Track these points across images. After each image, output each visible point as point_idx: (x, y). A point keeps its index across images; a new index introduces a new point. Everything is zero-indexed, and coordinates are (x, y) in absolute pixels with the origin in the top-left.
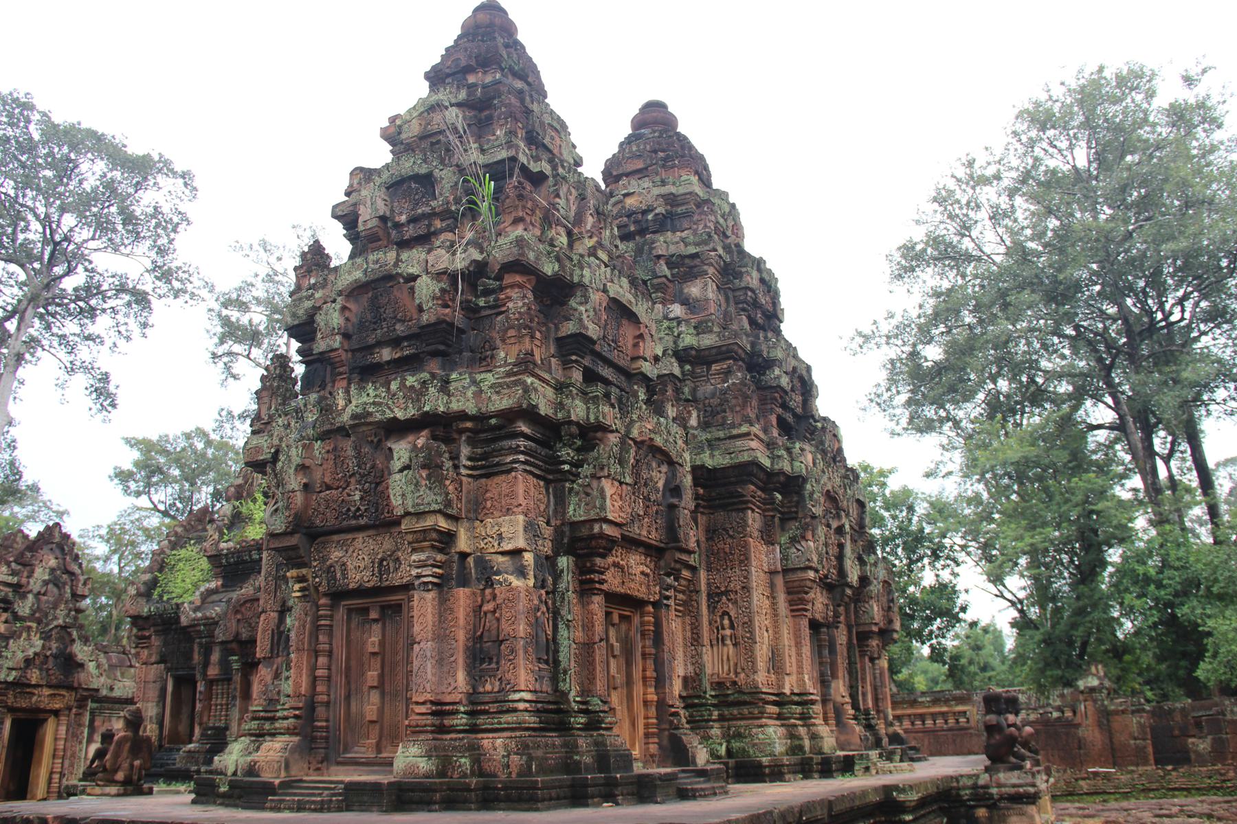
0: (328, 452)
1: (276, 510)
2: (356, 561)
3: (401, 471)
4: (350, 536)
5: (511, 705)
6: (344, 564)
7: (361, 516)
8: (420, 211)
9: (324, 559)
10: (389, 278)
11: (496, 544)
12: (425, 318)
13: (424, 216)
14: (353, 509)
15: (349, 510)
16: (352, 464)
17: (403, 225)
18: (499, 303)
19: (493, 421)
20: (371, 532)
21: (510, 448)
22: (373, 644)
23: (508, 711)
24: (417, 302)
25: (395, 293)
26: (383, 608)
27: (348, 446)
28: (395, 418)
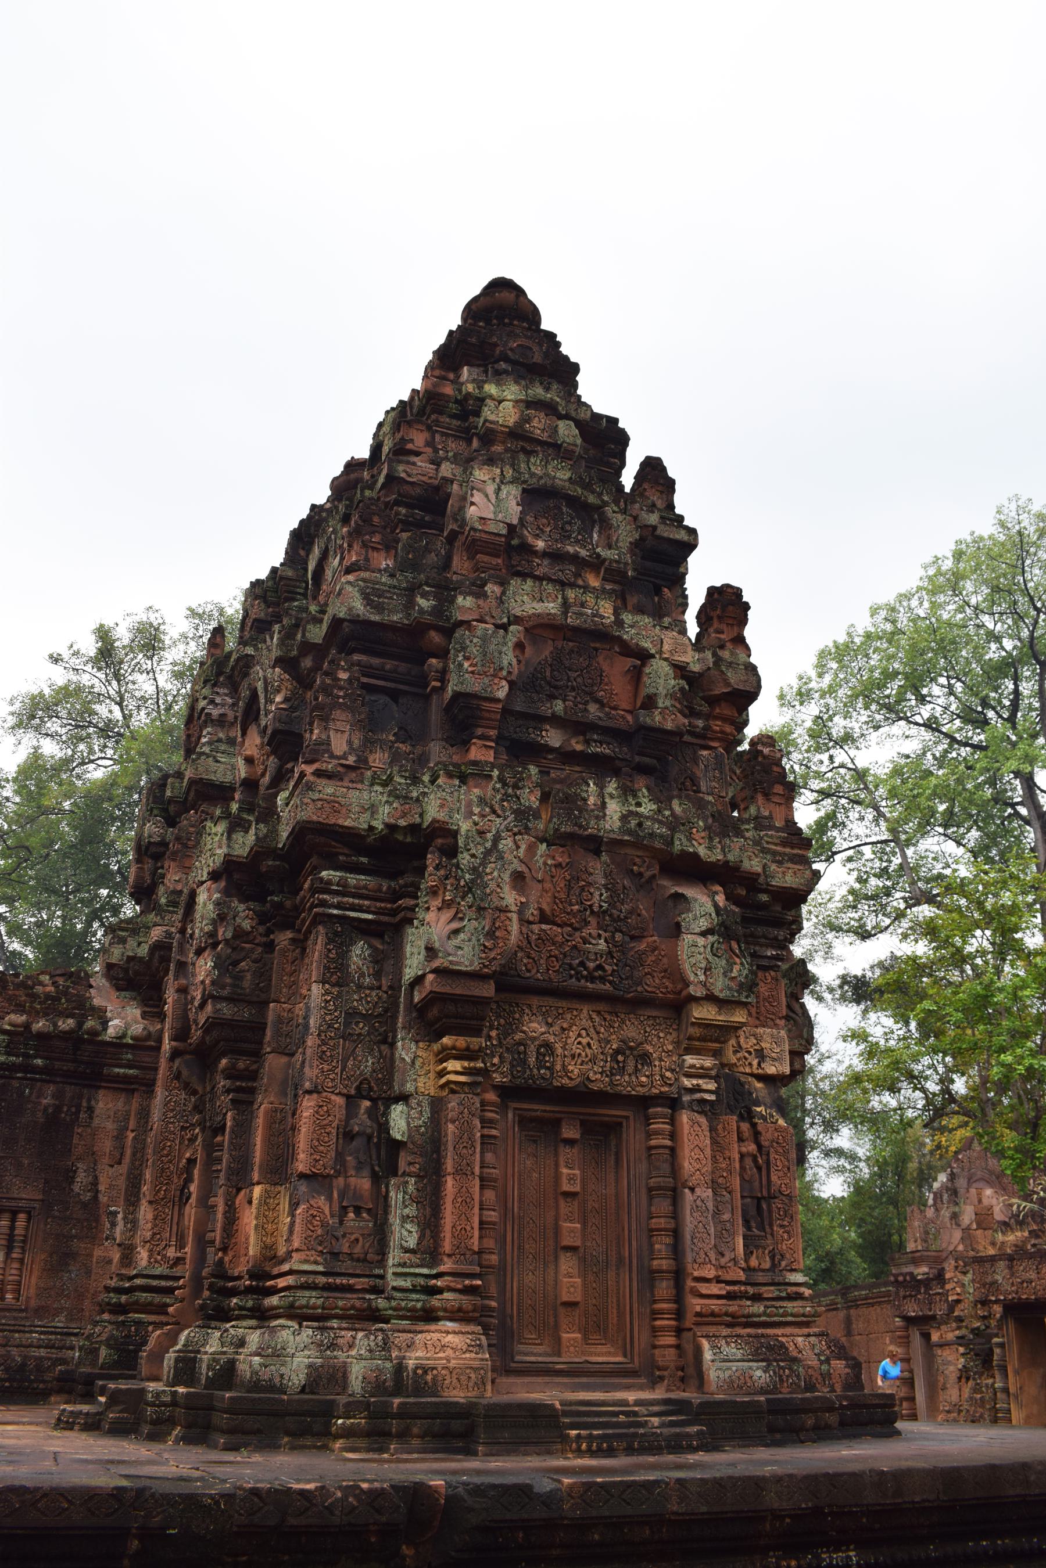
0: (559, 866)
1: (456, 932)
2: (576, 1046)
3: (703, 934)
4: (564, 1004)
5: (794, 1289)
6: (547, 1045)
7: (603, 979)
8: (571, 549)
9: (506, 1031)
10: (601, 637)
11: (755, 1062)
12: (656, 719)
13: (575, 558)
14: (591, 965)
15: (582, 964)
16: (598, 898)
17: (535, 553)
18: (709, 735)
19: (764, 898)
20: (601, 1007)
21: (776, 938)
22: (571, 1179)
23: (790, 1298)
24: (644, 692)
25: (600, 659)
26: (589, 1128)
27: (597, 869)
28: (695, 855)
